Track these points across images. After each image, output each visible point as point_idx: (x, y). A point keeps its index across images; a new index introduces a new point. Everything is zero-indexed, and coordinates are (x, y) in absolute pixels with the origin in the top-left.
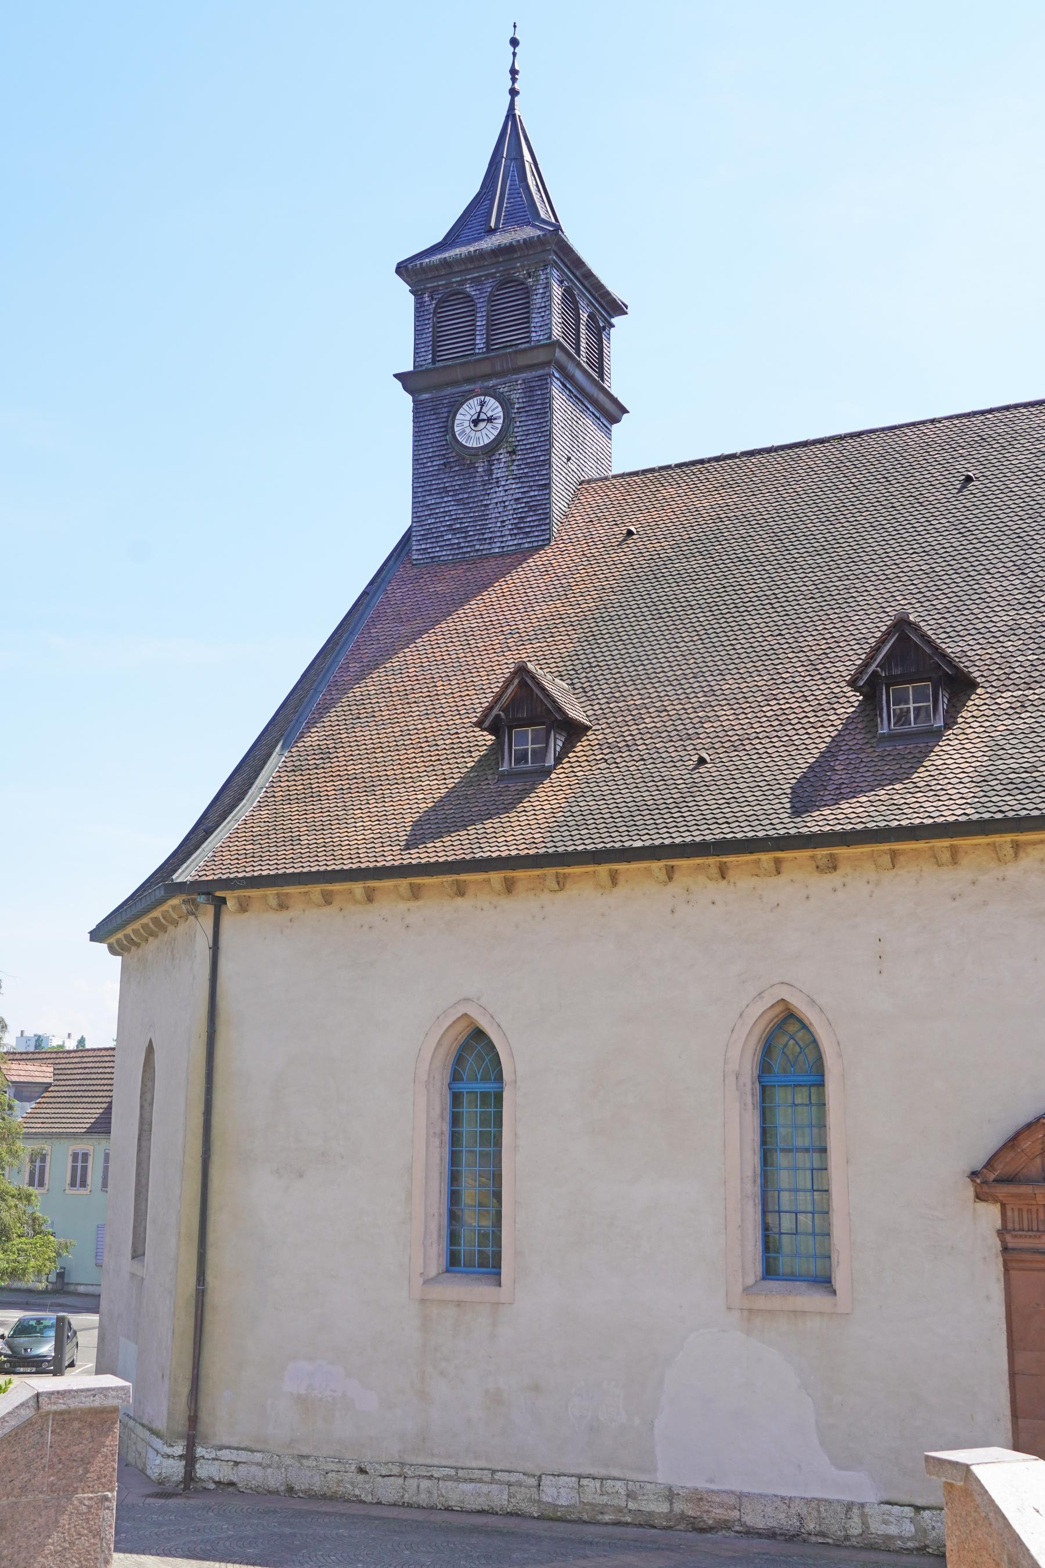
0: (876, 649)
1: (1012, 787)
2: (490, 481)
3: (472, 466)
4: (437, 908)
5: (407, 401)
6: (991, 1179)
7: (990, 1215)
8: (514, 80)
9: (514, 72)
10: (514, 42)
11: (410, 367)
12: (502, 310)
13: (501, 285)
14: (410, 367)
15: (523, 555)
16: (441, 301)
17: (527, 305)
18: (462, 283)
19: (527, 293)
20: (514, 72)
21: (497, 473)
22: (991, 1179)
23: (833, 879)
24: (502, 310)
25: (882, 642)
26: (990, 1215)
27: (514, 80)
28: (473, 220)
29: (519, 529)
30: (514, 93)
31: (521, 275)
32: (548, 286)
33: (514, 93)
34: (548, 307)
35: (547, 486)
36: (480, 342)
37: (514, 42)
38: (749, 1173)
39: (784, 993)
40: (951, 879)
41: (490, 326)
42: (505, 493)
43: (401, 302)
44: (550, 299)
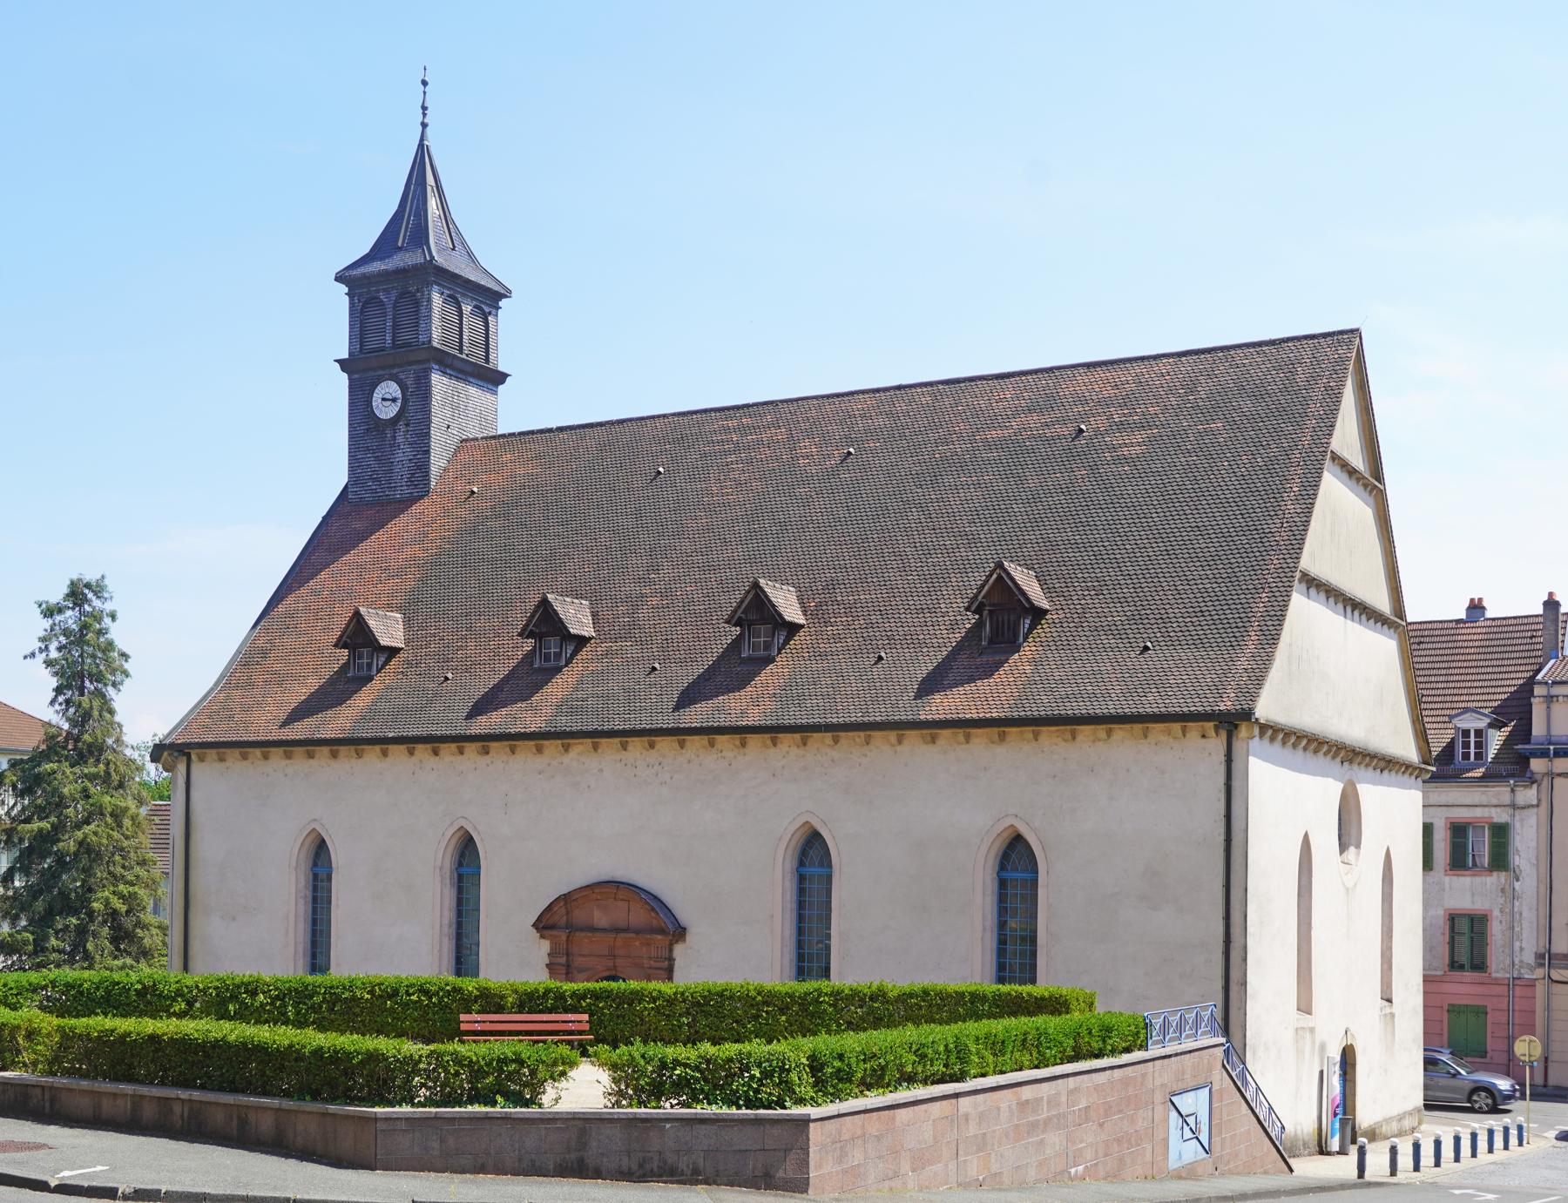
0: (533, 616)
1: (573, 711)
2: (394, 446)
3: (383, 432)
4: (299, 764)
5: (344, 379)
6: (544, 925)
7: (545, 946)
8: (424, 115)
9: (424, 108)
10: (424, 83)
11: (346, 356)
12: (409, 310)
13: (401, 296)
14: (346, 356)
15: (413, 500)
16: (366, 303)
17: (417, 312)
18: (378, 291)
19: (417, 303)
20: (424, 108)
21: (400, 439)
22: (544, 925)
23: (487, 759)
24: (409, 310)
25: (535, 612)
26: (545, 946)
27: (424, 115)
28: (385, 244)
29: (411, 482)
30: (424, 125)
31: (413, 289)
32: (429, 300)
33: (424, 125)
34: (429, 317)
35: (428, 452)
36: (389, 338)
37: (424, 83)
38: (446, 921)
39: (463, 823)
40: (539, 762)
41: (395, 327)
42: (403, 455)
43: (339, 300)
44: (430, 309)
